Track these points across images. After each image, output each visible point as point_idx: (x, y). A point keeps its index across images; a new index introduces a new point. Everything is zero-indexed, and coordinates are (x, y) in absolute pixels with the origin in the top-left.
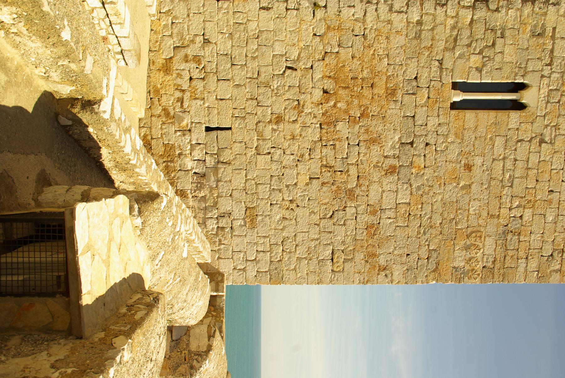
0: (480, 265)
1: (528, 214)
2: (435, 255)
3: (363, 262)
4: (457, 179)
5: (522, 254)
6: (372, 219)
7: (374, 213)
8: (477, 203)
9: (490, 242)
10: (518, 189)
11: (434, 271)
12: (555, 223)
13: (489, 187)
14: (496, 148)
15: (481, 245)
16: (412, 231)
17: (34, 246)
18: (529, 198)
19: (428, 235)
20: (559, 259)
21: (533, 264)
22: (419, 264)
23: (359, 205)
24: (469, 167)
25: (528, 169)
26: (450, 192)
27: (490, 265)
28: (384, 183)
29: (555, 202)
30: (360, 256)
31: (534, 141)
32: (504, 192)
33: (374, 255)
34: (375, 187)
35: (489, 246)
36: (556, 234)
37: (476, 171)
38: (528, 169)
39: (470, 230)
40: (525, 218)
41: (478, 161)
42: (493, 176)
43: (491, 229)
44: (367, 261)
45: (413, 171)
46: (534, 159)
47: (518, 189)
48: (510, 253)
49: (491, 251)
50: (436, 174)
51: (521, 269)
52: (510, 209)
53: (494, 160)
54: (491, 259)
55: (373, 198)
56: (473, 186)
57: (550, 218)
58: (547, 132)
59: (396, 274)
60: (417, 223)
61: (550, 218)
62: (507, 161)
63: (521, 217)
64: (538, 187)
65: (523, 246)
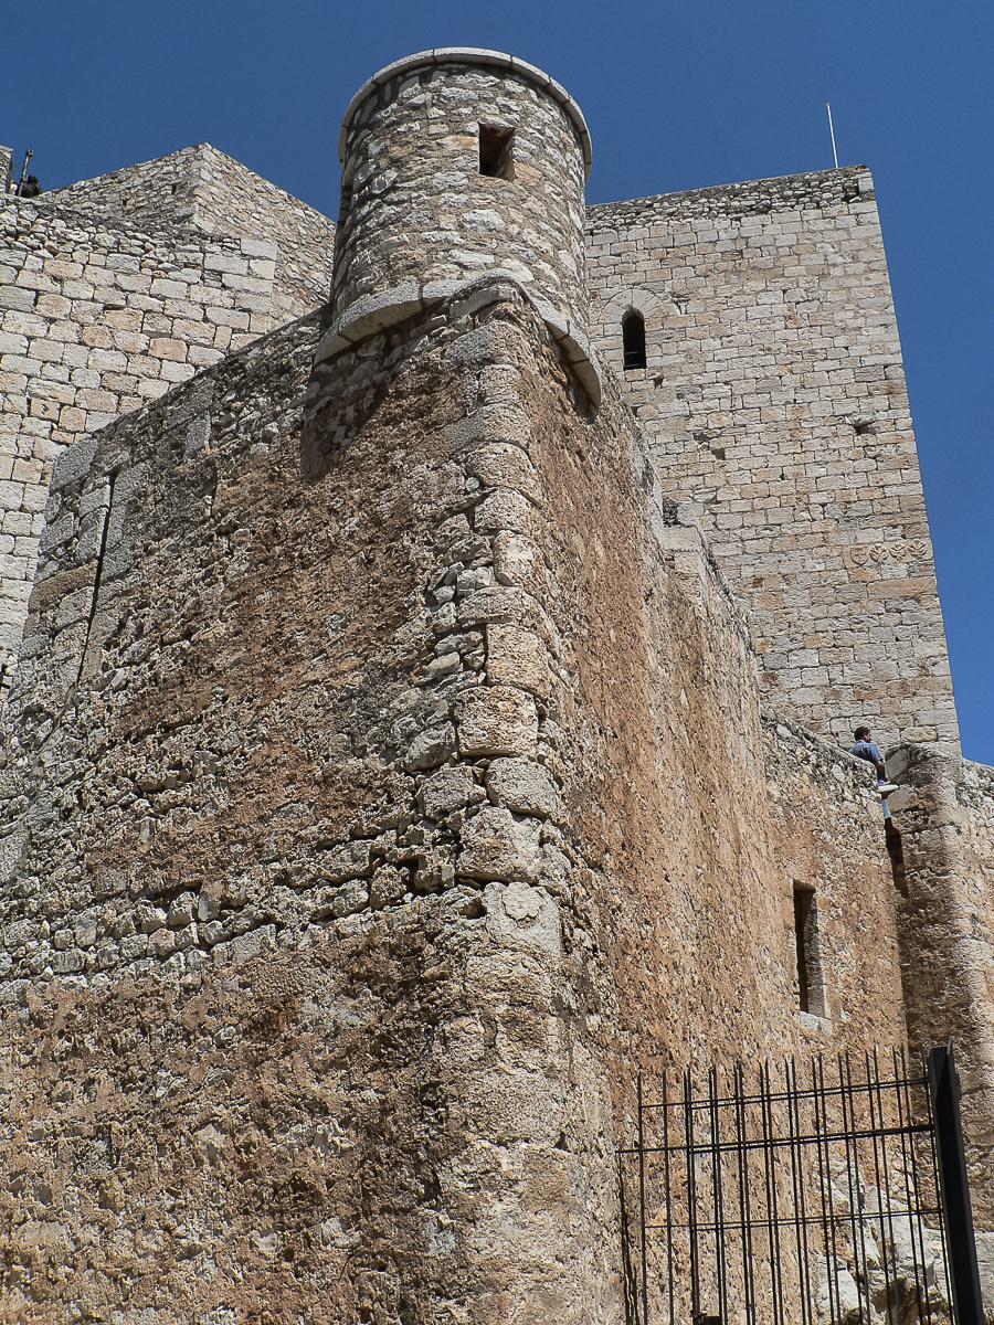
0: (902, 542)
1: (816, 498)
2: (893, 604)
3: (916, 699)
4: (776, 592)
5: (877, 494)
6: (847, 695)
7: (837, 694)
8: (809, 563)
9: (863, 537)
10: (784, 516)
11: (919, 602)
12: (827, 463)
13: (783, 552)
14: (728, 553)
15: (872, 547)
16: (859, 639)
17: (939, 1211)
18: (794, 502)
19: (863, 618)
20: (878, 449)
21: (893, 477)
22: (909, 622)
23: (827, 715)
24: (758, 582)
25: (753, 511)
26: (797, 599)
27: (899, 531)
28: (792, 685)
29: (796, 469)
30: (908, 705)
31: (716, 510)
32: (790, 532)
33: (904, 685)
34: (797, 697)
35: (870, 536)
36: (842, 458)
37: (762, 572)
38: (753, 511)
39: (849, 564)
40: (824, 499)
41: (748, 572)
42: (768, 549)
43: (845, 539)
44: (914, 694)
45: (768, 651)
46: (740, 506)
47: (784, 516)
48: (878, 508)
49: (879, 533)
50: (771, 621)
51: (900, 490)
52: (814, 520)
53: (744, 553)
54: (891, 530)
55: (815, 697)
56: (783, 572)
57: (822, 471)
58: (701, 498)
59: (929, 652)
60: (847, 637)
61: (822, 471)
62: (744, 537)
63: (823, 505)
64: (778, 494)
65: (864, 494)
